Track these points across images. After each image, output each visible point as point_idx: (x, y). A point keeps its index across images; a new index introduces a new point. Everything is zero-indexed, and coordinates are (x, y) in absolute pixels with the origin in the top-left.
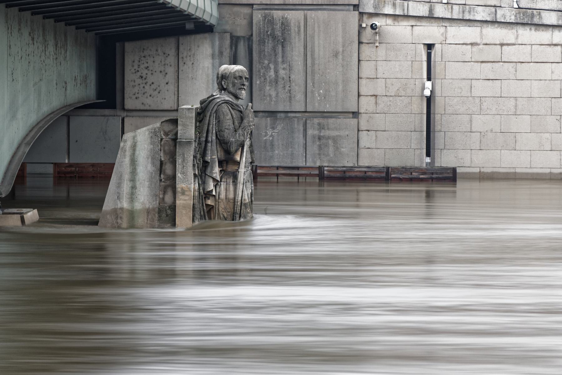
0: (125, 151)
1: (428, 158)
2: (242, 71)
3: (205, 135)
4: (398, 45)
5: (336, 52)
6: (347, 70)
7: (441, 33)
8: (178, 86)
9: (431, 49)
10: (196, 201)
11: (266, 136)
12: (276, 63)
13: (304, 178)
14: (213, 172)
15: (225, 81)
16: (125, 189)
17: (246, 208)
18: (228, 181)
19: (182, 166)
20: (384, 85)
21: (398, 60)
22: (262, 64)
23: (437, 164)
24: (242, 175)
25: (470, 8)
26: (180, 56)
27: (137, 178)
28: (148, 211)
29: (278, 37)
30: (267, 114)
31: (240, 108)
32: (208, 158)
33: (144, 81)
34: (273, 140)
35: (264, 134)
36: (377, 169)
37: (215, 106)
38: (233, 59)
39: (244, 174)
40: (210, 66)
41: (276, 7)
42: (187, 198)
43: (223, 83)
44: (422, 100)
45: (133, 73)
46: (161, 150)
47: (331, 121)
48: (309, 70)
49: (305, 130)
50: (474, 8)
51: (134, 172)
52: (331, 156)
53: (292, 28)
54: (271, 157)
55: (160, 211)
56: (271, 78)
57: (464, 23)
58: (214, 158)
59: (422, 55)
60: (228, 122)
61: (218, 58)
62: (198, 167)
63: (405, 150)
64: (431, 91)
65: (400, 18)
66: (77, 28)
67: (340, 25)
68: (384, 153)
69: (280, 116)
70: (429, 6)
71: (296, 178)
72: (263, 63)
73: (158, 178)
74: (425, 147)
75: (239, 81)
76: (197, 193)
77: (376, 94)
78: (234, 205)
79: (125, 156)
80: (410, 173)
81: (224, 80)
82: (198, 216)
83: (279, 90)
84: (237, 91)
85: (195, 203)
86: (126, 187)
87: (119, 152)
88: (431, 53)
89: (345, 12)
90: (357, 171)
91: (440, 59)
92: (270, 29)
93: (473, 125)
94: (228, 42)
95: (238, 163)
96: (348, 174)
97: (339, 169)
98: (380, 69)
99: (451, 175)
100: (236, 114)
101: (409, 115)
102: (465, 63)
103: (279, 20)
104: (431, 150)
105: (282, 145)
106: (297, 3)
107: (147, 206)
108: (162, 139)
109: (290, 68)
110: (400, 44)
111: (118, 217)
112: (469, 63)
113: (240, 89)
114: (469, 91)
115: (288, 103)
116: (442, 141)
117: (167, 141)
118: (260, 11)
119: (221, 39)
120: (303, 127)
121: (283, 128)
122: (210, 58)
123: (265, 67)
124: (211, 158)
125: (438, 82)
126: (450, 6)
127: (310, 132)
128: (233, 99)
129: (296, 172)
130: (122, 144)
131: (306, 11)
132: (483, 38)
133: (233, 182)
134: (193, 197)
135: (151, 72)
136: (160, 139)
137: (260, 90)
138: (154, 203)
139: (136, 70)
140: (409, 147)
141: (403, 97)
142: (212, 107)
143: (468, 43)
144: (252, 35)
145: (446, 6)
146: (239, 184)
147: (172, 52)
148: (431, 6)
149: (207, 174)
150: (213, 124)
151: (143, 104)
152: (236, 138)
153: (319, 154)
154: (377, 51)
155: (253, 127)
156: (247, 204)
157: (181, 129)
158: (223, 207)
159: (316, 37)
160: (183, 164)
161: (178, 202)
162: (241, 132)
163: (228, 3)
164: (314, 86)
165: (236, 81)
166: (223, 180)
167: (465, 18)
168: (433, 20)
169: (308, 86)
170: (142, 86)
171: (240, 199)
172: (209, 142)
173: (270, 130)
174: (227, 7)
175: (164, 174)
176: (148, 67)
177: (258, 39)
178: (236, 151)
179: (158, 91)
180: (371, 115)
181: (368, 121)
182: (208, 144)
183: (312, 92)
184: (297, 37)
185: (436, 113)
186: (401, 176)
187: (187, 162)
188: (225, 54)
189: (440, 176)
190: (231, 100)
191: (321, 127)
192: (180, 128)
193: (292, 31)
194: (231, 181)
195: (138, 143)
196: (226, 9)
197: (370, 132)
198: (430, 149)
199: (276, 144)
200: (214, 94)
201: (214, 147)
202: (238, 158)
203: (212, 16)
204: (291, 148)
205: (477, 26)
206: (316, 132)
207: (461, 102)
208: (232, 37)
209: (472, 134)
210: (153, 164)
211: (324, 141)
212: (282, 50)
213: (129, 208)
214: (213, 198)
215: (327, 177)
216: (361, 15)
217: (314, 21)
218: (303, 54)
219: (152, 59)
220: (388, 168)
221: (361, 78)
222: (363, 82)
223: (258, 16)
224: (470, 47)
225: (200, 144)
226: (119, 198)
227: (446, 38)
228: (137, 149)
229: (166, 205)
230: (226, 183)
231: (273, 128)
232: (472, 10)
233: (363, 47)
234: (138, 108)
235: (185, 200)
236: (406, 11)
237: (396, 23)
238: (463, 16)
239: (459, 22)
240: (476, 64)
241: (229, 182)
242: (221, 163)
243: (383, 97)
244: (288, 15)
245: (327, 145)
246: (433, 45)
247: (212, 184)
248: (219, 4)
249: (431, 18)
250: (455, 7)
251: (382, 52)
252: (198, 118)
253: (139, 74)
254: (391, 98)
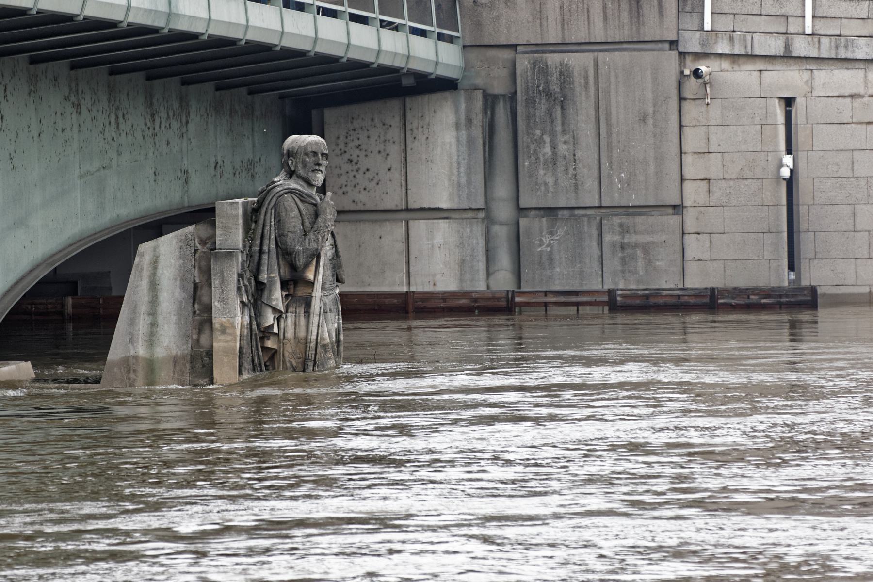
0: (142, 269)
1: (792, 273)
2: (317, 143)
3: (258, 242)
4: (739, 100)
5: (644, 113)
6: (661, 141)
7: (805, 80)
8: (406, 173)
9: (790, 106)
10: (245, 343)
11: (540, 245)
12: (553, 134)
13: (601, 308)
16: (141, 327)
17: (326, 352)
18: (298, 311)
20: (720, 163)
21: (741, 123)
22: (531, 136)
23: (805, 283)
24: (318, 301)
25: (847, 40)
26: (408, 127)
27: (159, 310)
28: (175, 360)
29: (555, 93)
30: (542, 212)
31: (314, 199)
32: (264, 277)
33: (355, 167)
34: (550, 251)
35: (537, 242)
36: (697, 292)
38: (489, 129)
40: (454, 141)
41: (551, 48)
42: (229, 338)
43: (290, 162)
44: (778, 184)
45: (337, 156)
46: (194, 267)
47: (639, 220)
48: (603, 143)
49: (600, 235)
50: (853, 40)
51: (154, 302)
52: (641, 273)
53: (576, 80)
54: (550, 278)
55: (193, 360)
56: (546, 157)
57: (839, 64)
58: (273, 277)
59: (776, 115)
60: (293, 222)
61: (464, 128)
62: (247, 291)
63: (755, 261)
64: (791, 171)
65: (741, 60)
66: (218, 89)
67: (649, 73)
68: (723, 266)
69: (563, 215)
70: (784, 40)
71: (575, 308)
72: (534, 135)
73: (190, 309)
74: (786, 257)
75: (313, 159)
76: (246, 331)
77: (708, 176)
78: (306, 347)
79: (141, 277)
80: (746, 297)
82: (247, 365)
83: (560, 175)
85: (242, 346)
86: (142, 325)
87: (133, 272)
88: (791, 110)
89: (655, 53)
90: (666, 296)
91: (805, 120)
92: (542, 82)
93: (857, 221)
94: (479, 104)
95: (311, 284)
96: (652, 301)
97: (639, 292)
98: (713, 139)
99: (809, 298)
100: (308, 209)
101: (760, 207)
102: (843, 125)
103: (556, 68)
104: (795, 261)
105: (566, 258)
106: (583, 41)
107: (174, 352)
108: (196, 251)
109: (575, 141)
110: (741, 100)
111: (130, 370)
112: (849, 126)
113: (313, 171)
114: (850, 168)
115: (574, 195)
116: (811, 246)
117: (204, 252)
118: (526, 55)
119: (469, 100)
120: (598, 230)
121: (567, 233)
122: (453, 129)
123: (536, 140)
124: (269, 278)
125: (802, 156)
126: (816, 39)
127: (607, 238)
128: (303, 187)
129: (573, 299)
130: (137, 259)
131: (596, 54)
132: (869, 85)
134: (241, 336)
135: (364, 153)
136: (193, 251)
137: (531, 176)
138: (185, 347)
139: (343, 151)
140: (761, 257)
141: (750, 181)
143: (847, 94)
144: (515, 92)
145: (810, 38)
147: (396, 122)
148: (787, 38)
150: (270, 225)
151: (354, 201)
152: (305, 245)
153: (623, 272)
154: (707, 111)
155: (333, 228)
156: (328, 346)
157: (221, 235)
158: (290, 351)
159: (613, 92)
161: (215, 345)
162: (312, 236)
163: (478, 44)
164: (611, 167)
165: (308, 159)
166: (290, 310)
167: (839, 57)
168: (792, 61)
169: (603, 167)
170: (351, 174)
171: (314, 337)
172: (264, 253)
173: (547, 236)
174: (476, 51)
175: (200, 303)
176: (360, 145)
177: (524, 98)
178: (307, 265)
179: (375, 181)
180: (702, 209)
181: (697, 219)
183: (610, 177)
184: (584, 93)
185: (800, 203)
186: (733, 302)
187: (228, 284)
188: (475, 122)
189: (792, 300)
190: (299, 188)
191: (624, 230)
192: (218, 232)
193: (576, 84)
195: (160, 258)
196: (474, 54)
197: (701, 235)
198: (794, 259)
199: (557, 257)
200: (276, 180)
201: (274, 260)
202: (310, 276)
203: (439, 65)
204: (580, 262)
205: (859, 69)
206: (617, 238)
207: (838, 185)
208: (486, 95)
209: (856, 234)
210: (183, 287)
211: (629, 251)
212: (562, 113)
213: (147, 356)
214: (276, 338)
215: (622, 306)
216: (682, 57)
217: (609, 68)
218: (593, 120)
219: (366, 133)
220: (713, 290)
221: (685, 153)
222: (688, 159)
223: (523, 63)
224: (848, 100)
225: (250, 256)
226: (131, 341)
227: (812, 88)
228: (160, 266)
229: (202, 350)
231: (551, 233)
232: (849, 43)
233: (686, 105)
234: (347, 208)
235: (227, 342)
236: (749, 48)
237: (736, 68)
238: (837, 53)
239: (831, 62)
240: (859, 126)
242: (284, 285)
243: (720, 181)
244: (569, 60)
245: (633, 257)
246: (794, 99)
247: (272, 316)
248: (464, 46)
249: (788, 57)
250: (824, 40)
251: (715, 112)
252: (254, 217)
253: (346, 156)
254: (732, 183)
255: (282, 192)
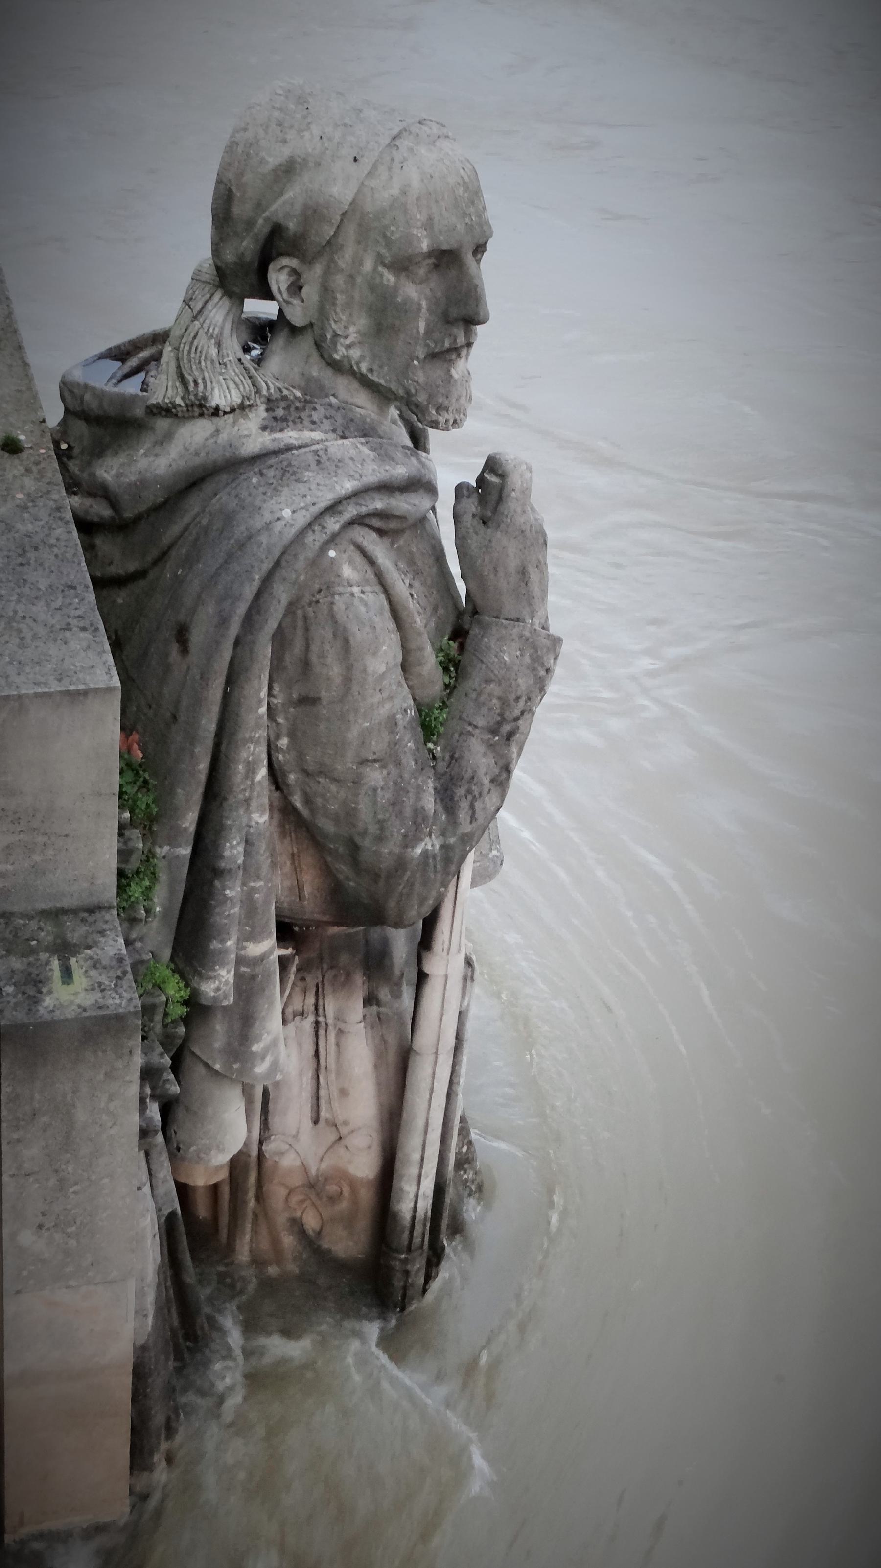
3: (189, 821)
14: (256, 1048)
15: (294, 272)
18: (330, 1006)
19: (53, 1182)
37: (267, 580)
39: (465, 979)
43: (278, 280)
58: (263, 958)
81: (293, 262)
84: (421, 377)
133: (370, 1000)
142: (249, 591)
146: (431, 1058)
149: (193, 1054)
160: (57, 1171)
182: (217, 883)
194: (356, 1009)
200: (219, 398)
230: (311, 1018)
241: (339, 1018)
255: (315, 539)
